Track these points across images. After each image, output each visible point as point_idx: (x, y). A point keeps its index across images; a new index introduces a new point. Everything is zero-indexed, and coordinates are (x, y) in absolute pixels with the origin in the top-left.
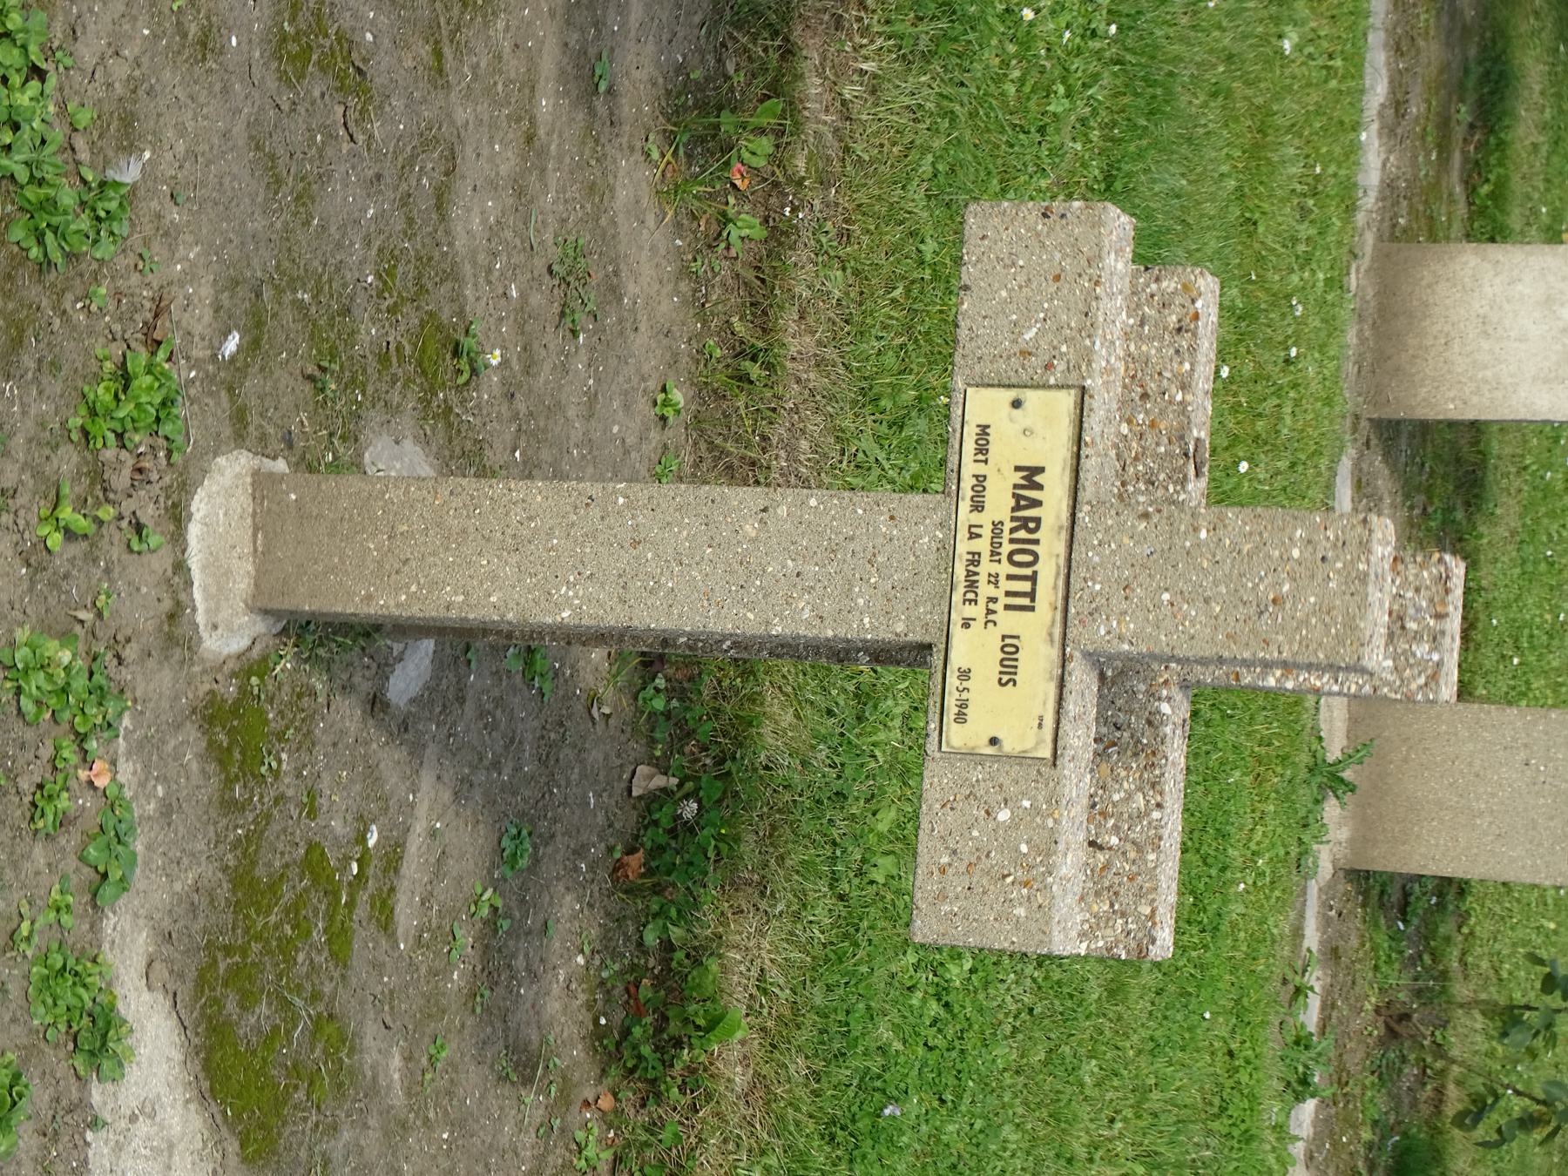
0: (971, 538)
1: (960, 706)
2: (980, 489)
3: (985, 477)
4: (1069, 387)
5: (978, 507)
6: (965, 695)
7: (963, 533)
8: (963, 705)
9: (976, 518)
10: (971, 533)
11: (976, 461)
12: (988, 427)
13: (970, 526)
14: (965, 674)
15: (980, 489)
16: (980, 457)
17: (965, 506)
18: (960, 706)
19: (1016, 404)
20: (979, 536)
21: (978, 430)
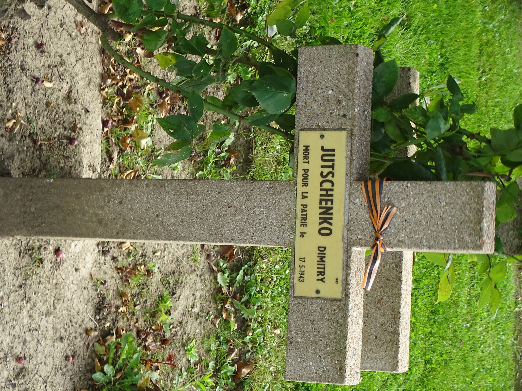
0: (303, 198)
1: (301, 274)
2: (306, 176)
3: (308, 170)
5: (305, 184)
6: (303, 269)
7: (299, 196)
8: (302, 273)
9: (305, 189)
10: (303, 196)
11: (304, 162)
12: (309, 146)
13: (303, 193)
14: (303, 260)
15: (306, 176)
16: (305, 160)
18: (301, 274)
19: (322, 136)
20: (307, 197)
21: (304, 148)
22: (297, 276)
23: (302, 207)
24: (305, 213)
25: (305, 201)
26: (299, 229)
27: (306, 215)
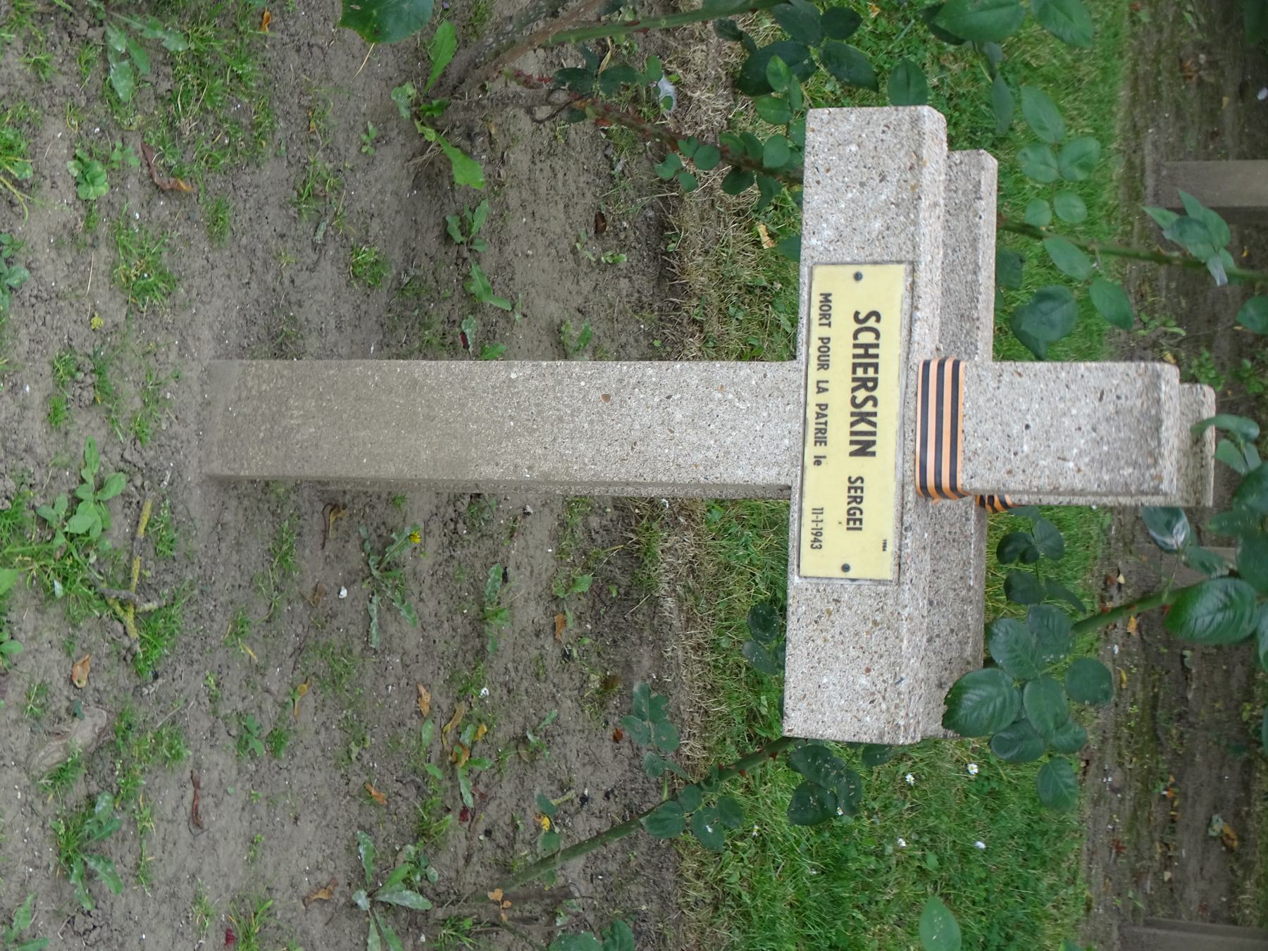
0: (819, 392)
3: (829, 339)
4: (900, 262)
5: (824, 365)
7: (812, 388)
9: (823, 375)
10: (819, 388)
13: (818, 382)
16: (824, 321)
17: (814, 363)
19: (858, 277)
20: (826, 390)
21: (821, 298)
22: (807, 538)
23: (817, 409)
24: (823, 420)
25: (822, 398)
26: (812, 450)
27: (826, 423)
